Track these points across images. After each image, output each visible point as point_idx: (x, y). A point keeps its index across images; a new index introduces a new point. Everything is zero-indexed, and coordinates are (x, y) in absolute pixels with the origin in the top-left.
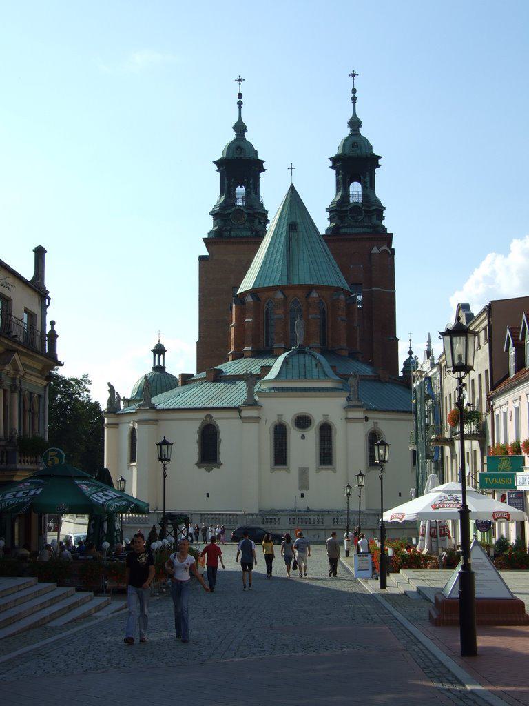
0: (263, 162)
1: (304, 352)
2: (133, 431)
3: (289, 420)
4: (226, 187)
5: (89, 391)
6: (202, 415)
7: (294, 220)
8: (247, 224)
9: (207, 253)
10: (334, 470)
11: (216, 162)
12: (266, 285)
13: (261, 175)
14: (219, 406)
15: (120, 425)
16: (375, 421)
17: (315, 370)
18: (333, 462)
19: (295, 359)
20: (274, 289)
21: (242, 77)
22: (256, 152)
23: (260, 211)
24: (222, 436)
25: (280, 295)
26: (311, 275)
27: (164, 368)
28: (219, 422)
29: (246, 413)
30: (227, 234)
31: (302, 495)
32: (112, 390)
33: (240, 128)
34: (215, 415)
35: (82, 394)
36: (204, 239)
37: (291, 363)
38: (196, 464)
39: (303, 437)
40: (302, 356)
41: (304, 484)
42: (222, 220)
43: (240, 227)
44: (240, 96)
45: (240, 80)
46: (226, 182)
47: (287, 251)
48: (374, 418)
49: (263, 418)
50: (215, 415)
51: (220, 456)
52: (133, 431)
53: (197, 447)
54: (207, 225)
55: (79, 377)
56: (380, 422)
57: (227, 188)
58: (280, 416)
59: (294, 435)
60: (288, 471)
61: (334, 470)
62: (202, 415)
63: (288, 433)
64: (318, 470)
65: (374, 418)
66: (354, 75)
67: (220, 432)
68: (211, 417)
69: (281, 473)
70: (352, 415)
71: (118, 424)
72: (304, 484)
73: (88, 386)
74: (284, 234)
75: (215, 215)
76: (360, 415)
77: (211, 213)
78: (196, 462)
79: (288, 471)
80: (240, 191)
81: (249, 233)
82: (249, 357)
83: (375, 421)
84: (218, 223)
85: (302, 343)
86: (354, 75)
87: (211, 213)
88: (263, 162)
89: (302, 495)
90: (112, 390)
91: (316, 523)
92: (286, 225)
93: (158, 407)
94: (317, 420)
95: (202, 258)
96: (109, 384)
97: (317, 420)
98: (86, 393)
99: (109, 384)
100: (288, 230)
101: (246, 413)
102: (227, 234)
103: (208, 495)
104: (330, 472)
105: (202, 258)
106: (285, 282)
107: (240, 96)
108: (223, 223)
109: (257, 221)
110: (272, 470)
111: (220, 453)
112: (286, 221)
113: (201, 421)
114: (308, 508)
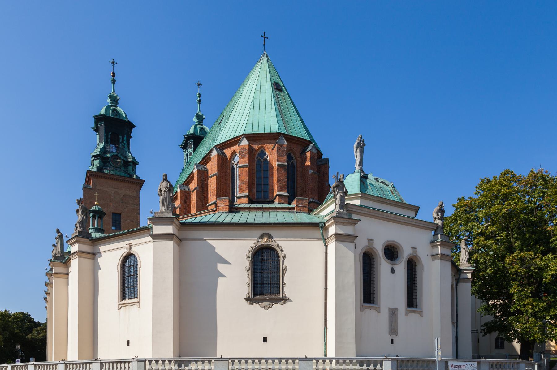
8: (123, 168)
18: (418, 304)
42: (103, 162)
43: (117, 169)
60: (378, 310)
79: (378, 310)
108: (103, 164)
109: (130, 168)
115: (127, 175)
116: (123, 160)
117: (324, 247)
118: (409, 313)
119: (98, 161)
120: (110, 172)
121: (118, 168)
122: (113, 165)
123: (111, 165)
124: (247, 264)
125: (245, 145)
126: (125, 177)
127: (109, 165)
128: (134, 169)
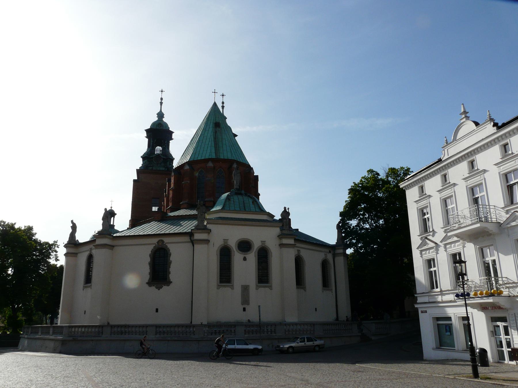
0: (173, 132)
1: (241, 194)
2: (90, 258)
3: (233, 244)
4: (151, 144)
5: (56, 252)
6: (155, 240)
7: (217, 121)
9: (136, 178)
10: (271, 287)
11: (147, 131)
12: (199, 158)
13: (170, 141)
14: (171, 232)
15: (79, 255)
16: (299, 249)
17: (252, 206)
19: (236, 198)
20: (206, 161)
21: (163, 90)
22: (169, 128)
23: (170, 157)
24: (173, 258)
25: (210, 164)
26: (232, 154)
27: (113, 226)
28: (169, 246)
29: (197, 236)
30: (150, 168)
31: (244, 309)
32: (74, 227)
33: (161, 115)
34: (166, 240)
35: (52, 253)
36: (137, 169)
37: (232, 200)
38: (147, 283)
39: (245, 259)
40: (240, 197)
41: (245, 300)
43: (158, 165)
44: (162, 99)
45: (162, 91)
46: (152, 141)
47: (214, 138)
48: (298, 247)
49: (211, 243)
50: (166, 240)
51: (170, 275)
52: (90, 258)
53: (149, 267)
54: (139, 163)
55: (51, 242)
56: (302, 250)
57: (151, 146)
58: (225, 241)
59: (237, 257)
61: (271, 287)
62: (155, 240)
63: (233, 254)
64: (257, 287)
65: (298, 247)
66: (223, 95)
67: (170, 255)
68: (163, 241)
69: (226, 291)
70: (285, 241)
71: (77, 254)
72: (245, 300)
73: (56, 248)
74: (211, 129)
75: (144, 158)
76: (292, 241)
77: (142, 157)
78: (147, 281)
80: (159, 149)
81: (164, 169)
82: (185, 209)
83: (299, 249)
84: (145, 162)
85: (238, 187)
86: (223, 95)
87: (142, 157)
88: (173, 132)
89: (244, 309)
90: (74, 227)
91: (269, 333)
92: (212, 124)
93: (114, 235)
94: (257, 245)
95: (134, 181)
96: (72, 222)
97: (257, 245)
98: (55, 253)
99: (72, 222)
100: (214, 126)
101: (197, 236)
102: (150, 168)
103: (157, 310)
104: (267, 289)
105: (134, 181)
106: (214, 156)
107: (162, 99)
109: (168, 163)
110: (219, 287)
111: (169, 273)
112: (212, 121)
113: (155, 245)
114: (249, 321)
115: (165, 169)
116: (163, 159)
117: (193, 247)
118: (259, 288)
119: (146, 161)
120: (152, 168)
121: (159, 164)
122: (155, 163)
123: (154, 163)
124: (149, 260)
125: (187, 169)
126: (163, 170)
127: (153, 163)
128: (171, 163)
